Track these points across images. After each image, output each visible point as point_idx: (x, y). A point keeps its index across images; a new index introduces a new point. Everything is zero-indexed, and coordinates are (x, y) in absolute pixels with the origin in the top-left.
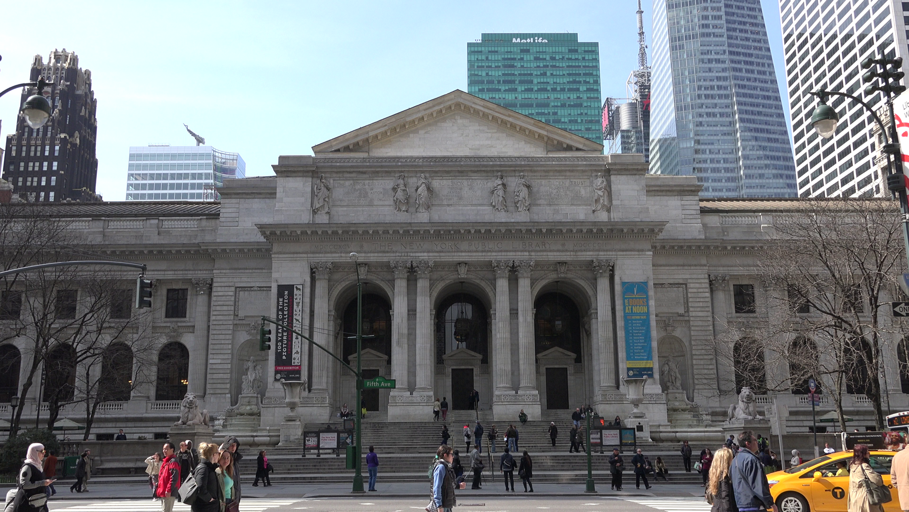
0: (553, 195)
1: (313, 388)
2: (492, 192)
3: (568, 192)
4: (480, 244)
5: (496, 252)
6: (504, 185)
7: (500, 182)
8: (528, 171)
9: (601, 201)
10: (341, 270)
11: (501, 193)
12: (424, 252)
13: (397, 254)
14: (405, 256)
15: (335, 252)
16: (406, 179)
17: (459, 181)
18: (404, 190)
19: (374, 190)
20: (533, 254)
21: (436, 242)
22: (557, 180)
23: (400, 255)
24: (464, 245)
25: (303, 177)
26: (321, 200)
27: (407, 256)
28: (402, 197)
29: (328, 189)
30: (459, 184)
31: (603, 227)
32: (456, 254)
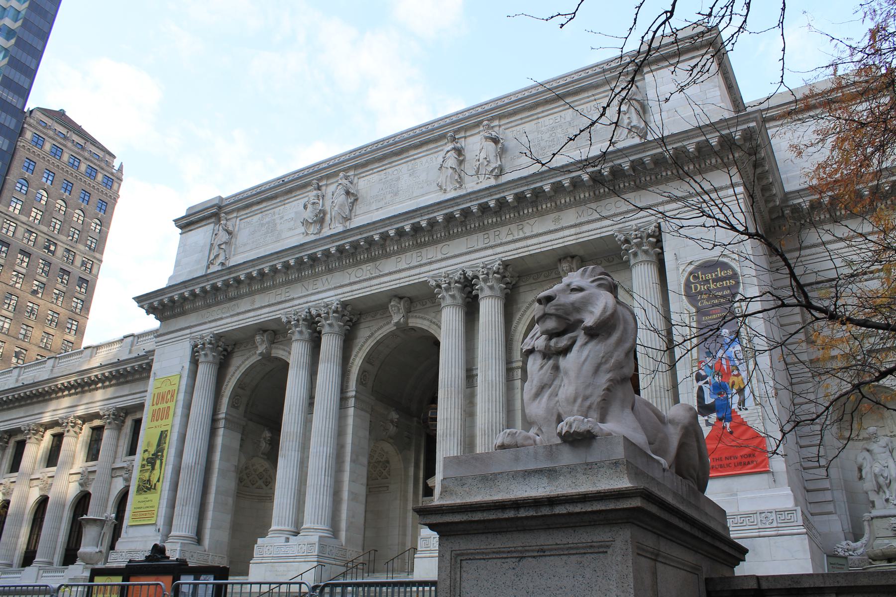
1: (173, 533)
4: (414, 255)
6: (459, 151)
7: (450, 146)
8: (500, 117)
9: (626, 121)
10: (243, 348)
11: (452, 162)
15: (221, 319)
16: (324, 188)
17: (396, 168)
18: (314, 204)
19: (286, 218)
25: (205, 225)
26: (217, 247)
27: (307, 303)
29: (230, 233)
30: (395, 172)
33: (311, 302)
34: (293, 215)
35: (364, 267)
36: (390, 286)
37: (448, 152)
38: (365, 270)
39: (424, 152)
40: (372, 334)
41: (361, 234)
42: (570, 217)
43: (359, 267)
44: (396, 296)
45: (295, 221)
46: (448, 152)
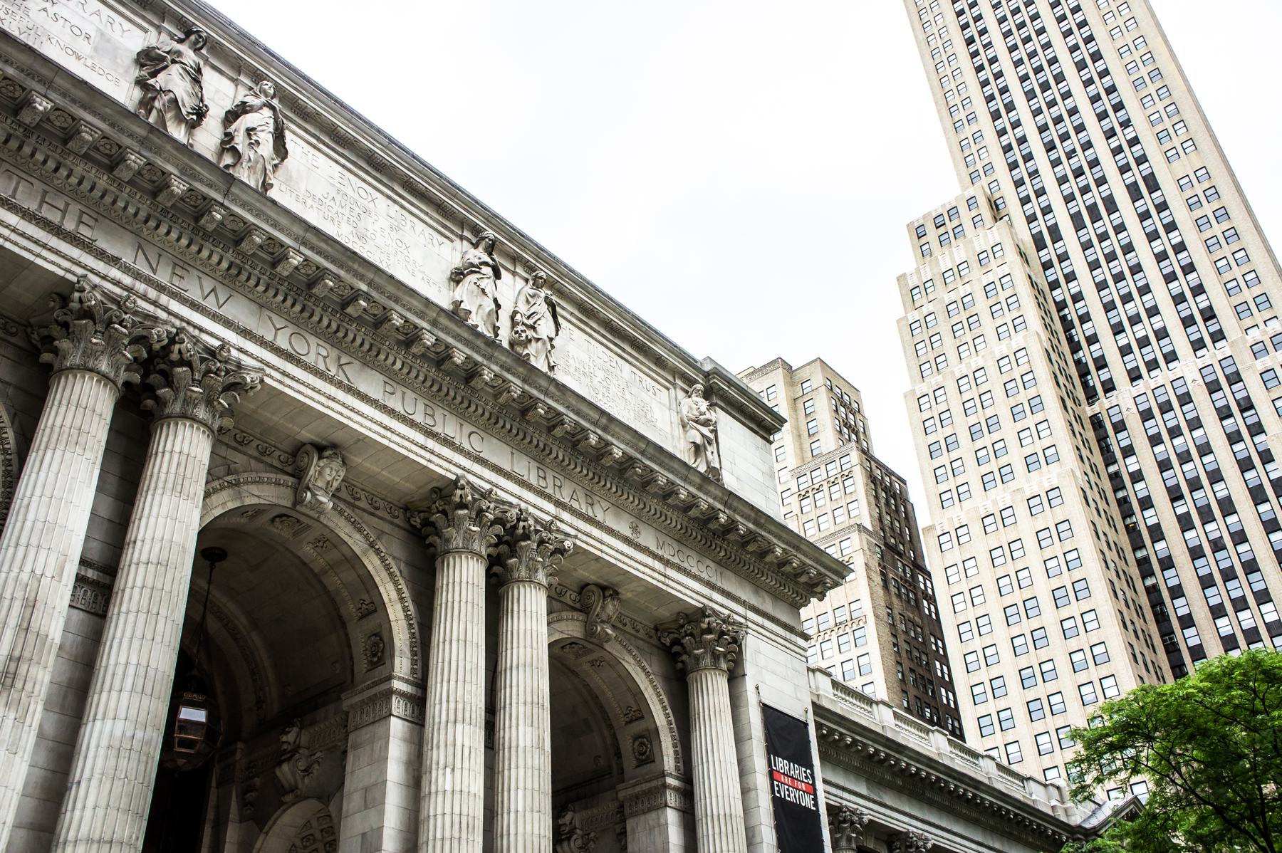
0: (595, 381)
2: (457, 277)
3: (628, 396)
4: (420, 407)
5: (467, 455)
12: (228, 324)
13: (114, 273)
14: (145, 298)
20: (566, 516)
21: (275, 317)
22: (605, 350)
23: (127, 280)
24: (372, 384)
27: (155, 303)
28: (186, 99)
30: (364, 195)
31: (739, 518)
32: (340, 395)
33: (166, 309)
34: (93, 34)
35: (313, 341)
36: (370, 430)
37: (486, 264)
38: (313, 347)
39: (421, 210)
40: (238, 484)
41: (369, 285)
42: (648, 538)
43: (303, 332)
44: (334, 446)
45: (96, 49)
46: (486, 264)
